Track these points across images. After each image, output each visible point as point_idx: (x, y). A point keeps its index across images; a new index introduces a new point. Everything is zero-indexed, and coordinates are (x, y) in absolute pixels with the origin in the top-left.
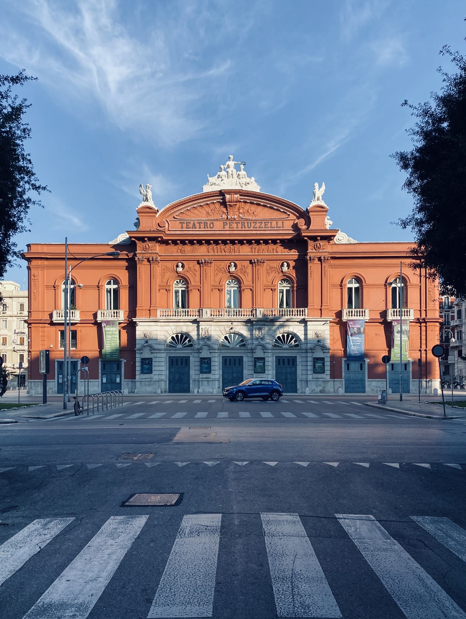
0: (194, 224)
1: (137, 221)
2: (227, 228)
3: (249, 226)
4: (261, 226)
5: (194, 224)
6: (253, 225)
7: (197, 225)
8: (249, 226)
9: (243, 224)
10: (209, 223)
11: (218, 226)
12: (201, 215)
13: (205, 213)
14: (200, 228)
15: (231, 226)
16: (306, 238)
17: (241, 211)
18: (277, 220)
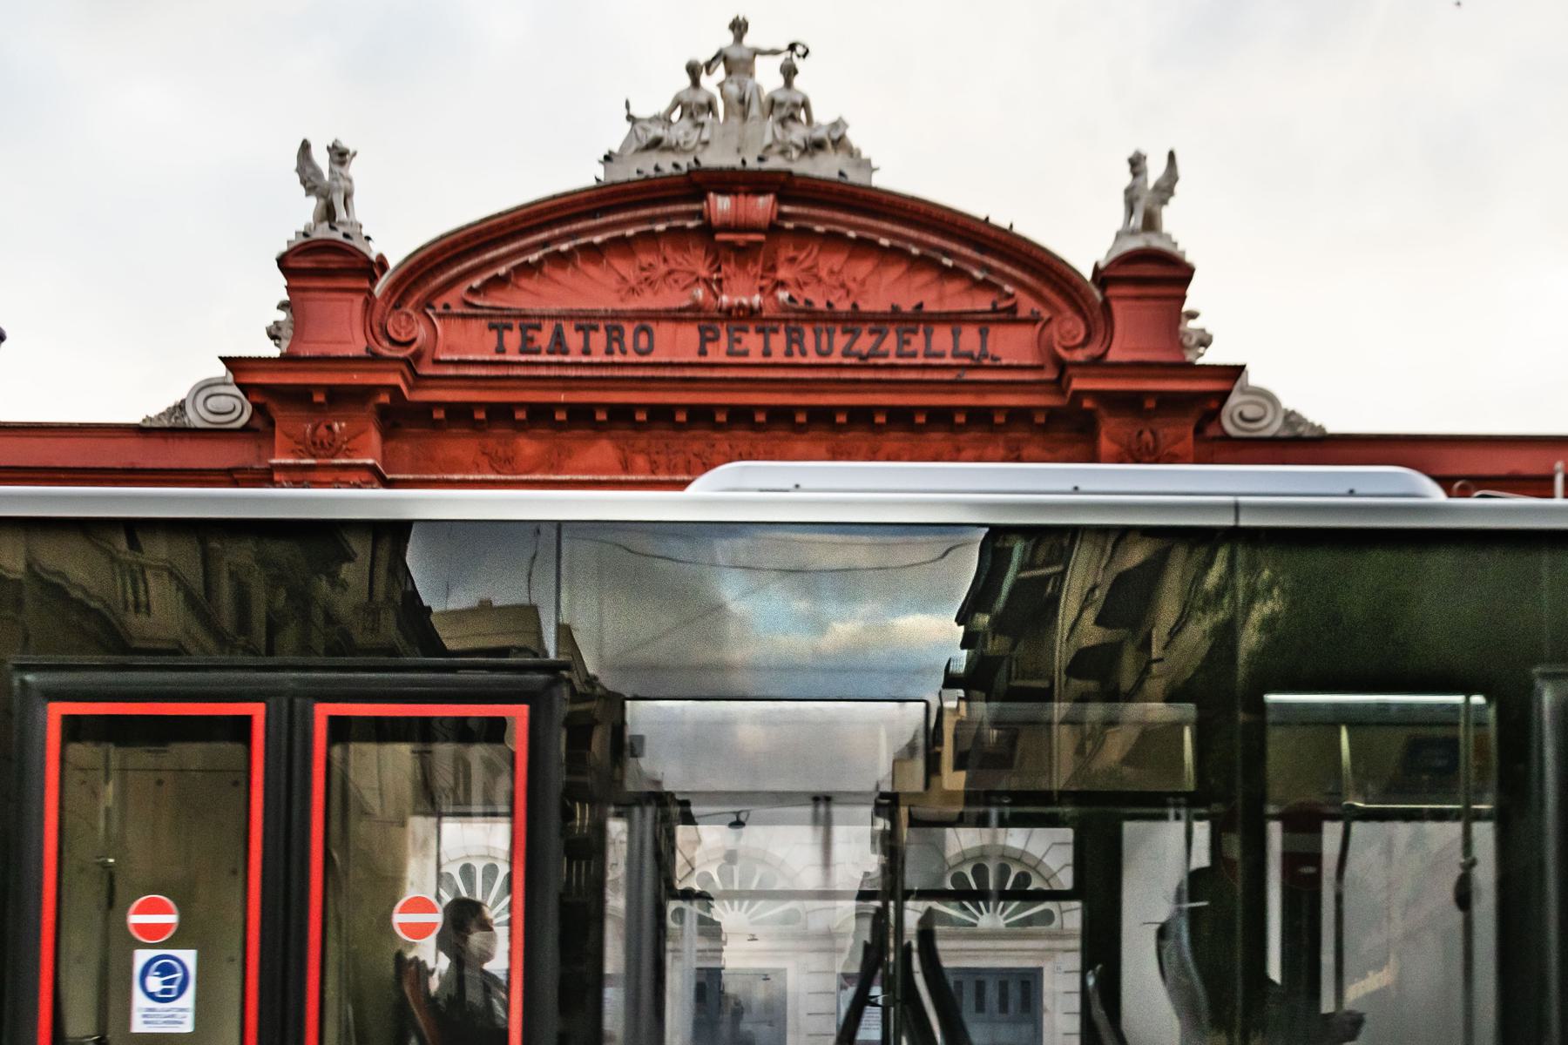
0: (558, 335)
1: (282, 316)
2: (717, 353)
3: (824, 346)
4: (883, 348)
5: (558, 335)
6: (841, 341)
7: (574, 339)
8: (824, 346)
9: (794, 339)
10: (629, 330)
11: (677, 345)
12: (596, 289)
13: (612, 281)
14: (586, 352)
15: (737, 347)
16: (1087, 404)
17: (783, 273)
18: (955, 320)
